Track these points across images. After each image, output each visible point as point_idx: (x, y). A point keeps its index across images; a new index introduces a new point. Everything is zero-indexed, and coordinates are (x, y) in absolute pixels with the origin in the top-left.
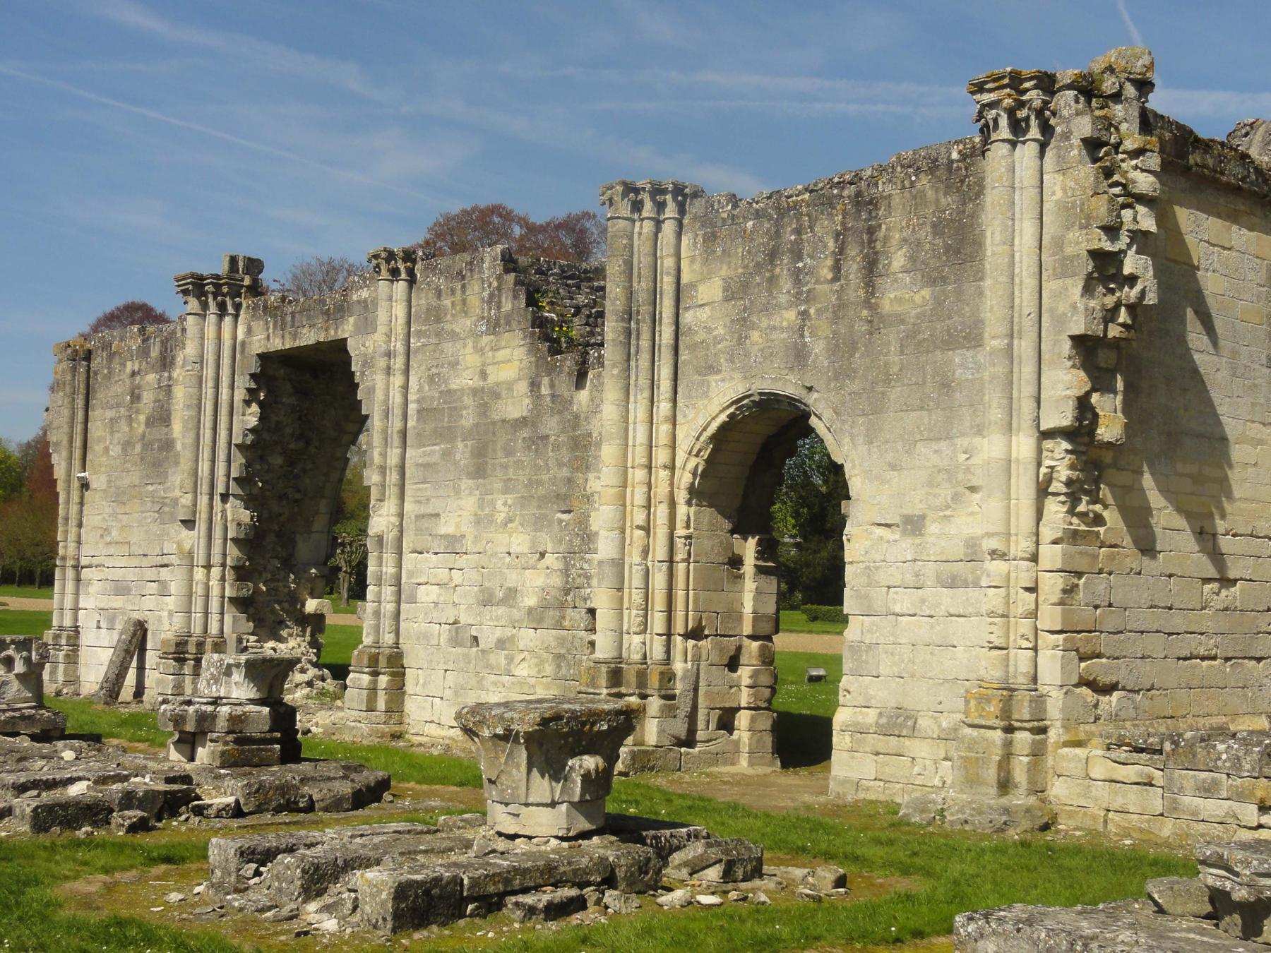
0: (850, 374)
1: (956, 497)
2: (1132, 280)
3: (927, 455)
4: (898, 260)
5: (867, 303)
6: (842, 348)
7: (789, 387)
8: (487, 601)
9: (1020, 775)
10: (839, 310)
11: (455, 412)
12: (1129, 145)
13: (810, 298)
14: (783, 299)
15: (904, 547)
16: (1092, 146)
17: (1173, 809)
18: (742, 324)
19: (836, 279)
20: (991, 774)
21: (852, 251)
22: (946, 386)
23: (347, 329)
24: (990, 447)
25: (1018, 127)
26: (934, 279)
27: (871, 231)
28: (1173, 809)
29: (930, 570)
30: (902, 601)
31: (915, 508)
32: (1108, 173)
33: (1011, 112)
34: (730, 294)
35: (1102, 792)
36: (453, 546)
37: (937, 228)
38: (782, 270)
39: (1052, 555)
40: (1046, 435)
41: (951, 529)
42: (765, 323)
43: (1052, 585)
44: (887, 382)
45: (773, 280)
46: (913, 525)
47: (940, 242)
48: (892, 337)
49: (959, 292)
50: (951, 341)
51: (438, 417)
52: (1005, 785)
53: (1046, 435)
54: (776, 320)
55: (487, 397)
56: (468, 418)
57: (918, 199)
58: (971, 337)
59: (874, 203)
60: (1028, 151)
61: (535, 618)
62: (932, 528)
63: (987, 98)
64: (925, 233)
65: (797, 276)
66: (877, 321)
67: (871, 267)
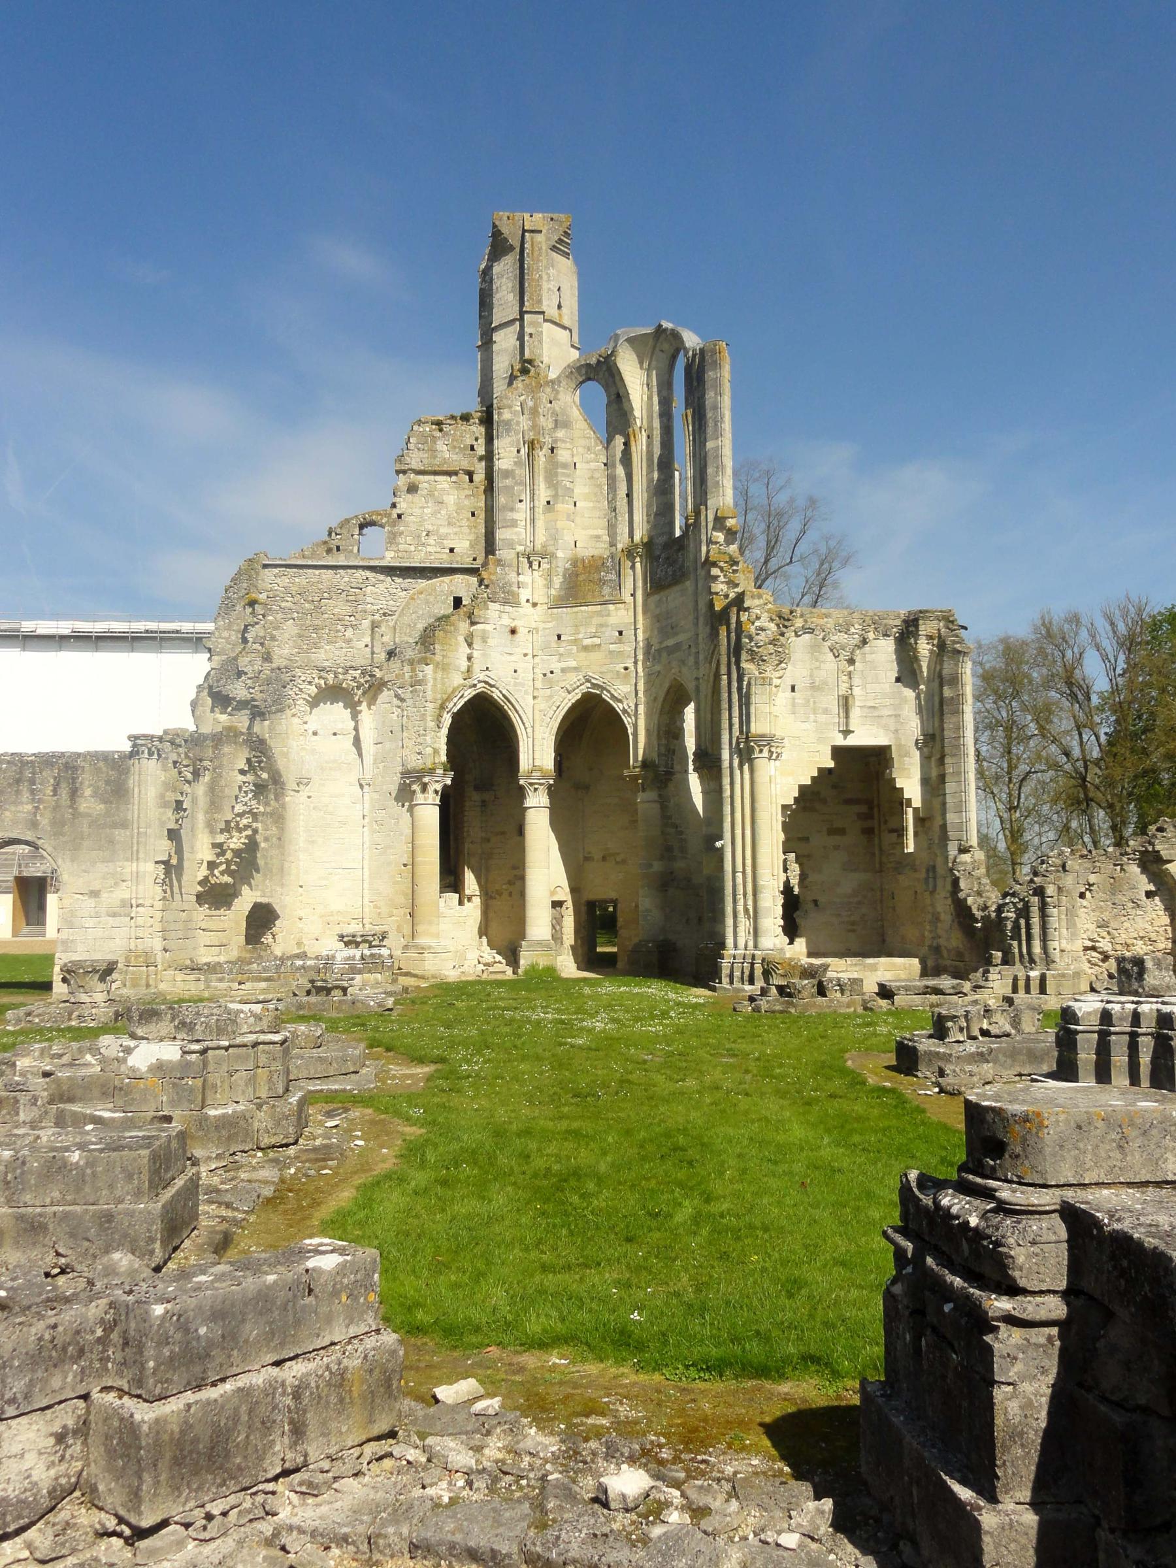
0: (63, 835)
1: (116, 884)
2: (185, 810)
3: (102, 868)
4: (88, 792)
5: (71, 807)
6: (58, 825)
9: (151, 982)
10: (56, 808)
12: (184, 763)
13: (40, 801)
14: (24, 800)
15: (92, 902)
16: (175, 763)
17: (208, 987)
19: (55, 795)
20: (143, 982)
21: (63, 785)
22: (111, 842)
24: (130, 868)
25: (151, 754)
26: (105, 802)
27: (74, 779)
28: (208, 987)
29: (103, 911)
30: (90, 923)
31: (97, 887)
32: (180, 773)
33: (149, 749)
35: (181, 985)
37: (107, 783)
38: (24, 787)
39: (159, 905)
40: (157, 862)
41: (114, 895)
42: (13, 808)
43: (159, 915)
44: (82, 839)
45: (18, 792)
46: (95, 894)
47: (108, 788)
48: (85, 823)
49: (118, 808)
50: (115, 826)
52: (148, 986)
53: (157, 862)
54: (20, 808)
57: (98, 770)
58: (124, 825)
59: (75, 768)
60: (153, 762)
62: (104, 895)
63: (139, 742)
64: (101, 784)
65: (32, 792)
66: (76, 814)
67: (74, 793)
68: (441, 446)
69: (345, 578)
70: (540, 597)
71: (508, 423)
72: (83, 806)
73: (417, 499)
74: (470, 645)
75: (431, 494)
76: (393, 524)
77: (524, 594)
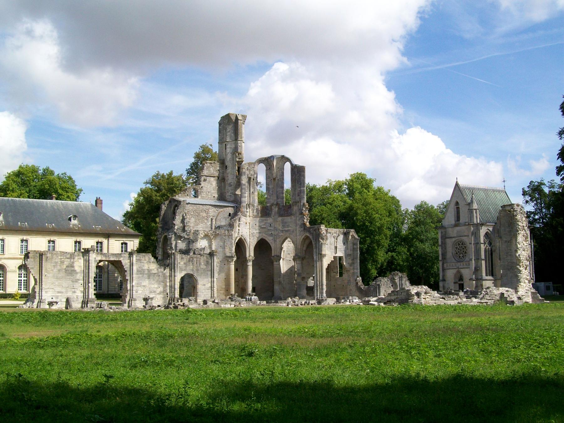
6: (198, 270)
7: (191, 273)
8: (151, 292)
11: (144, 272)
15: (204, 287)
18: (186, 267)
23: (121, 259)
34: (184, 264)
36: (144, 286)
46: (205, 285)
51: (141, 271)
55: (149, 270)
56: (146, 272)
61: (159, 294)
67: (200, 264)
68: (211, 169)
69: (205, 207)
70: (251, 215)
71: (245, 172)
72: (202, 267)
73: (206, 183)
74: (239, 226)
75: (209, 181)
76: (200, 189)
77: (248, 214)
